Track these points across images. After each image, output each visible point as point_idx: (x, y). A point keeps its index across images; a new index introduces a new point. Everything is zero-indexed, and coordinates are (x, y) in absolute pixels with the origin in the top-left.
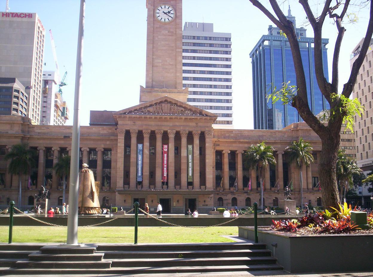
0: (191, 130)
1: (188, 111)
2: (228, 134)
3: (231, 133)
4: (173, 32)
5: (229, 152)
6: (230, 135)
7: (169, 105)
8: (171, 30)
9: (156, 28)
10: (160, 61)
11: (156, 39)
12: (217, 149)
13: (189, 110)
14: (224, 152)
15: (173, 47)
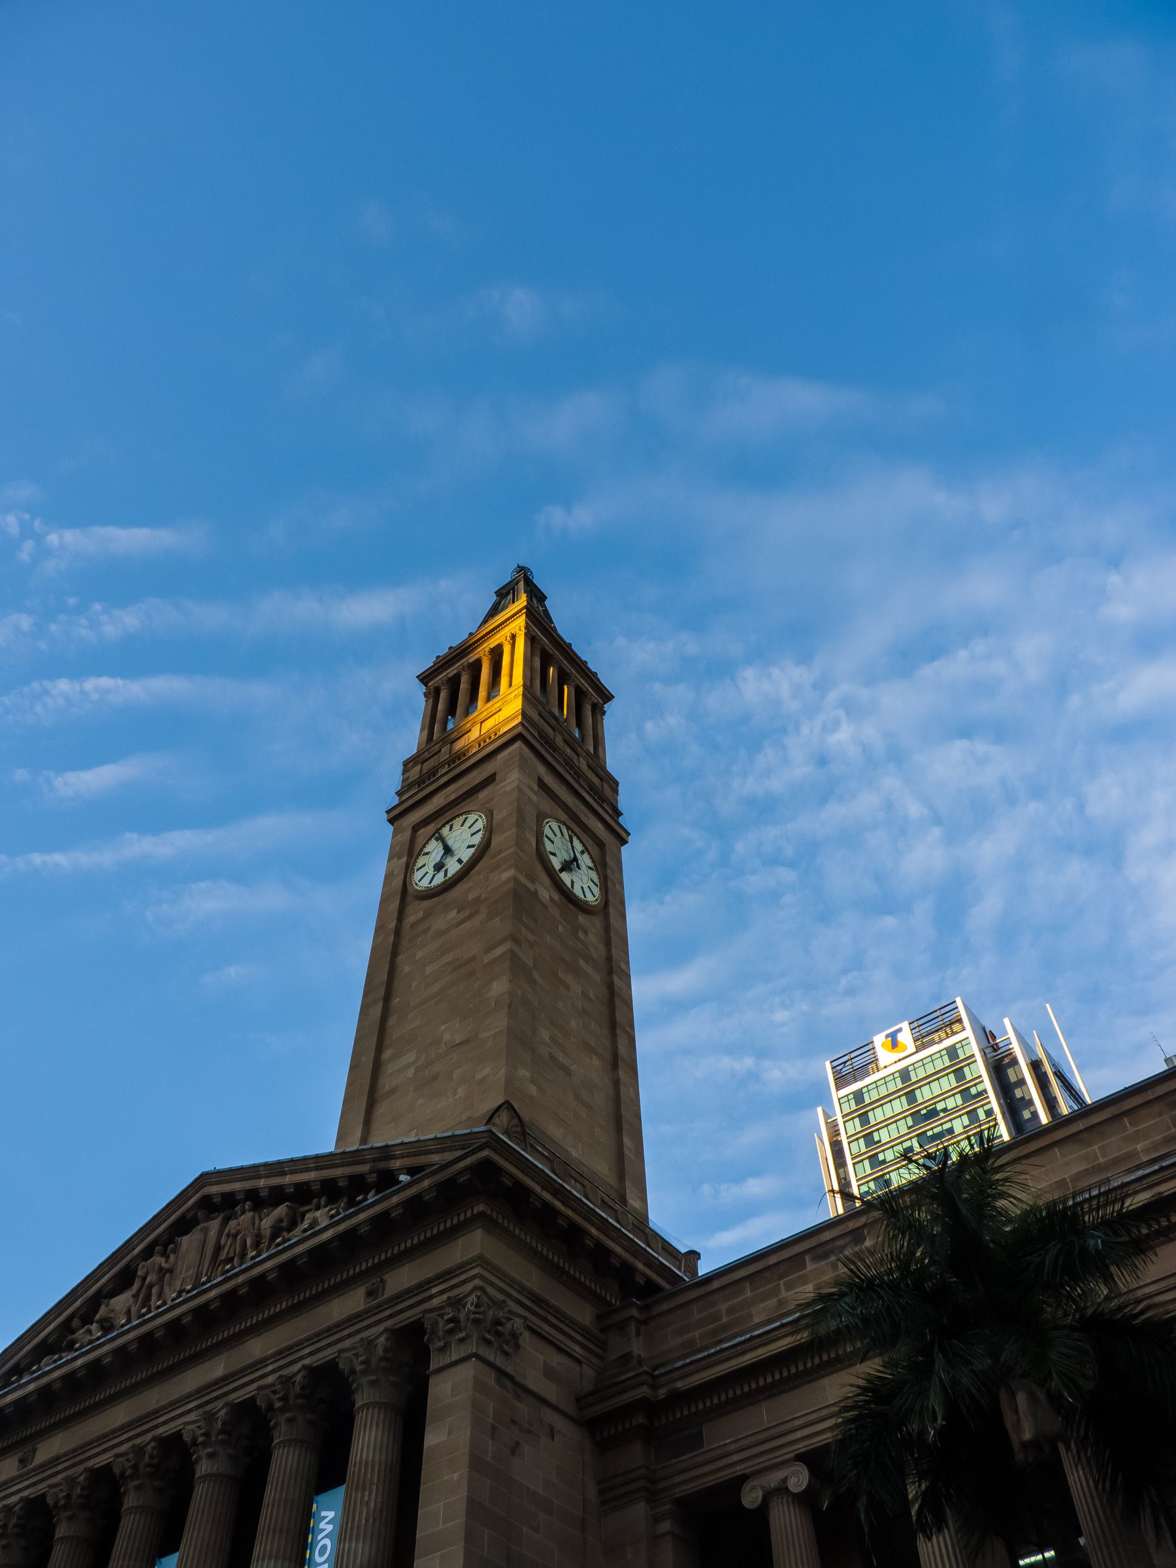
0: (329, 1354)
1: (318, 1208)
2: (763, 1298)
3: (789, 1287)
4: (478, 900)
5: (799, 1479)
6: (781, 1303)
7: (214, 1225)
8: (471, 897)
9: (413, 926)
10: (410, 1057)
11: (407, 969)
12: (679, 1492)
13: (323, 1201)
14: (751, 1498)
15: (474, 958)
